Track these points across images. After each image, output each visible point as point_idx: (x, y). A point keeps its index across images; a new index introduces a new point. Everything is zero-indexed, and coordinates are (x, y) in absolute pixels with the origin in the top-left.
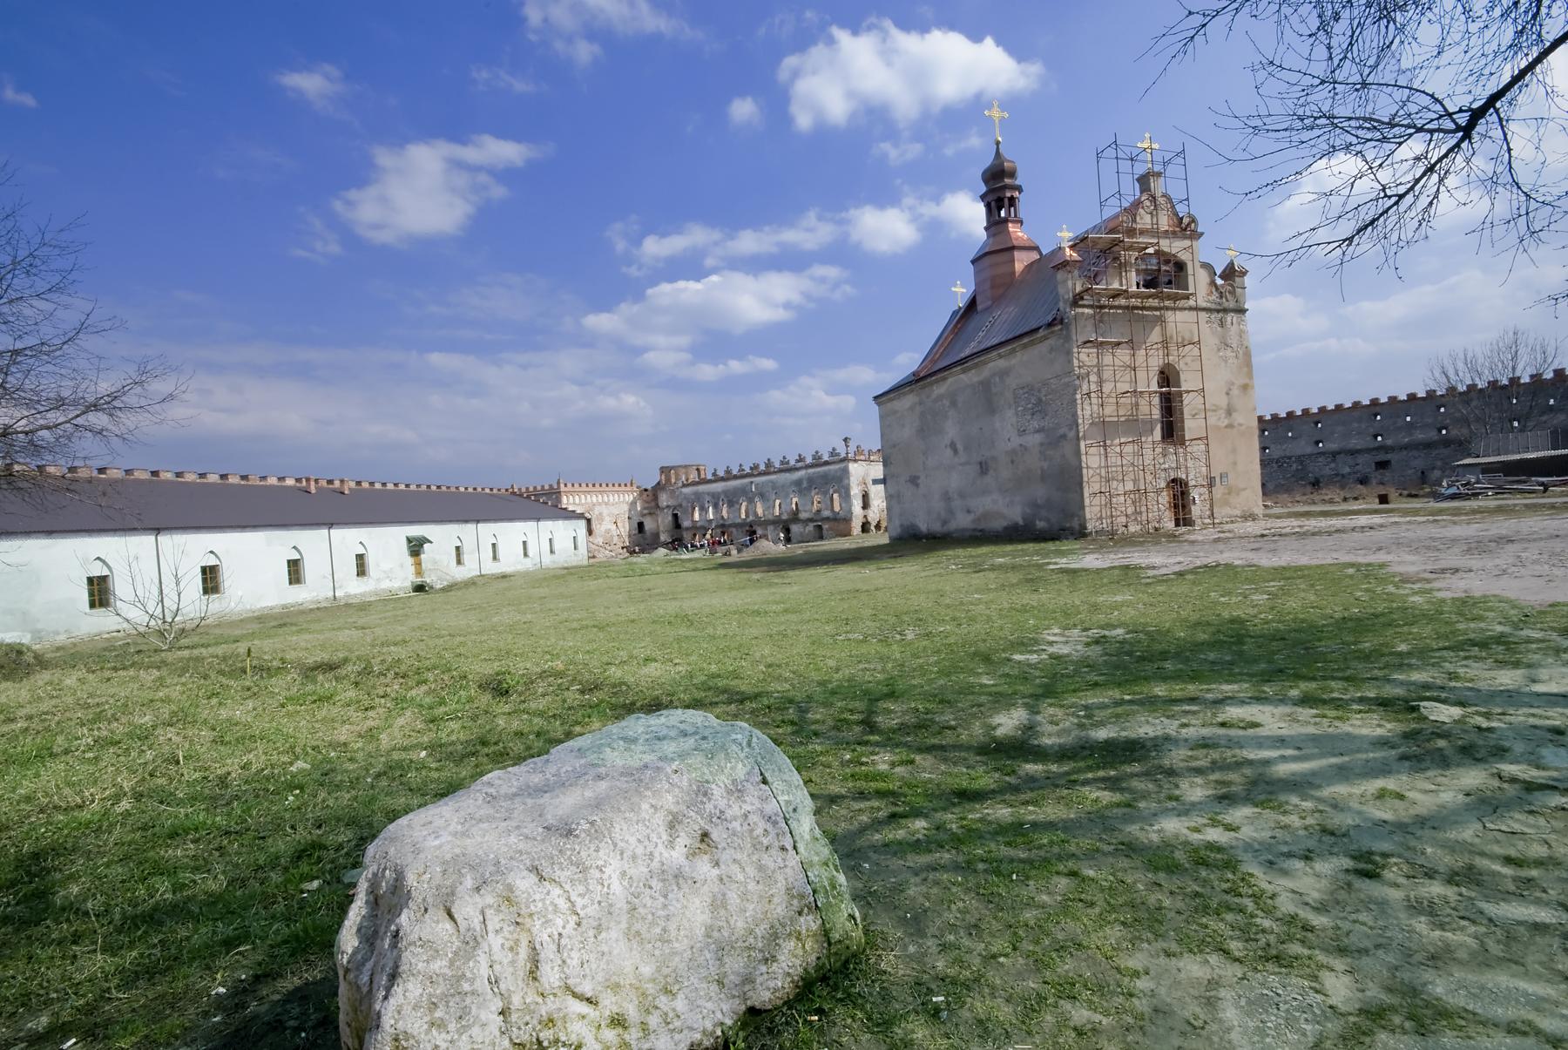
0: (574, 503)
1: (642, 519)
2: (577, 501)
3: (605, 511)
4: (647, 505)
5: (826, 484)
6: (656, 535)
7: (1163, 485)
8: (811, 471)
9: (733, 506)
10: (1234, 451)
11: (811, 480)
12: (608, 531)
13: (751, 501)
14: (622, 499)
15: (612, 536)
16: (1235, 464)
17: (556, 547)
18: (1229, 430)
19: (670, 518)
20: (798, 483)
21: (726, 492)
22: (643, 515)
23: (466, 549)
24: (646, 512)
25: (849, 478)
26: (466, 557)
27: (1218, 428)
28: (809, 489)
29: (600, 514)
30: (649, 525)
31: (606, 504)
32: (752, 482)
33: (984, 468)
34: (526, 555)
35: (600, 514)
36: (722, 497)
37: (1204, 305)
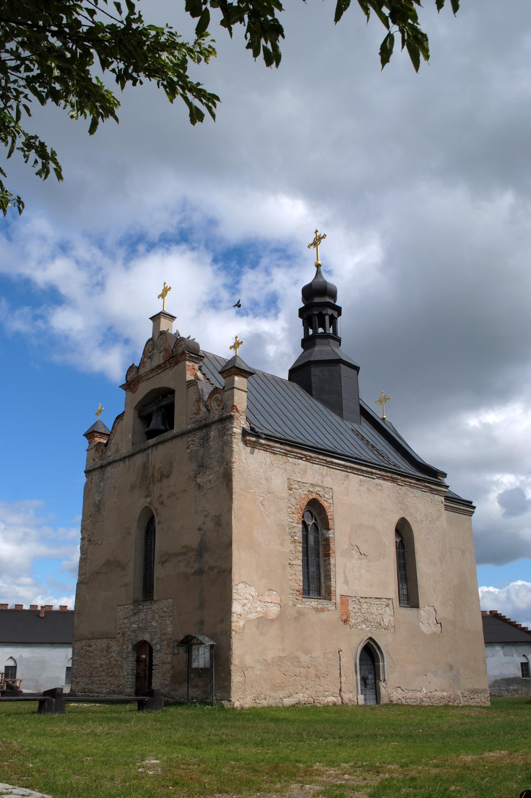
7: (130, 647)
16: (202, 623)
37: (189, 427)
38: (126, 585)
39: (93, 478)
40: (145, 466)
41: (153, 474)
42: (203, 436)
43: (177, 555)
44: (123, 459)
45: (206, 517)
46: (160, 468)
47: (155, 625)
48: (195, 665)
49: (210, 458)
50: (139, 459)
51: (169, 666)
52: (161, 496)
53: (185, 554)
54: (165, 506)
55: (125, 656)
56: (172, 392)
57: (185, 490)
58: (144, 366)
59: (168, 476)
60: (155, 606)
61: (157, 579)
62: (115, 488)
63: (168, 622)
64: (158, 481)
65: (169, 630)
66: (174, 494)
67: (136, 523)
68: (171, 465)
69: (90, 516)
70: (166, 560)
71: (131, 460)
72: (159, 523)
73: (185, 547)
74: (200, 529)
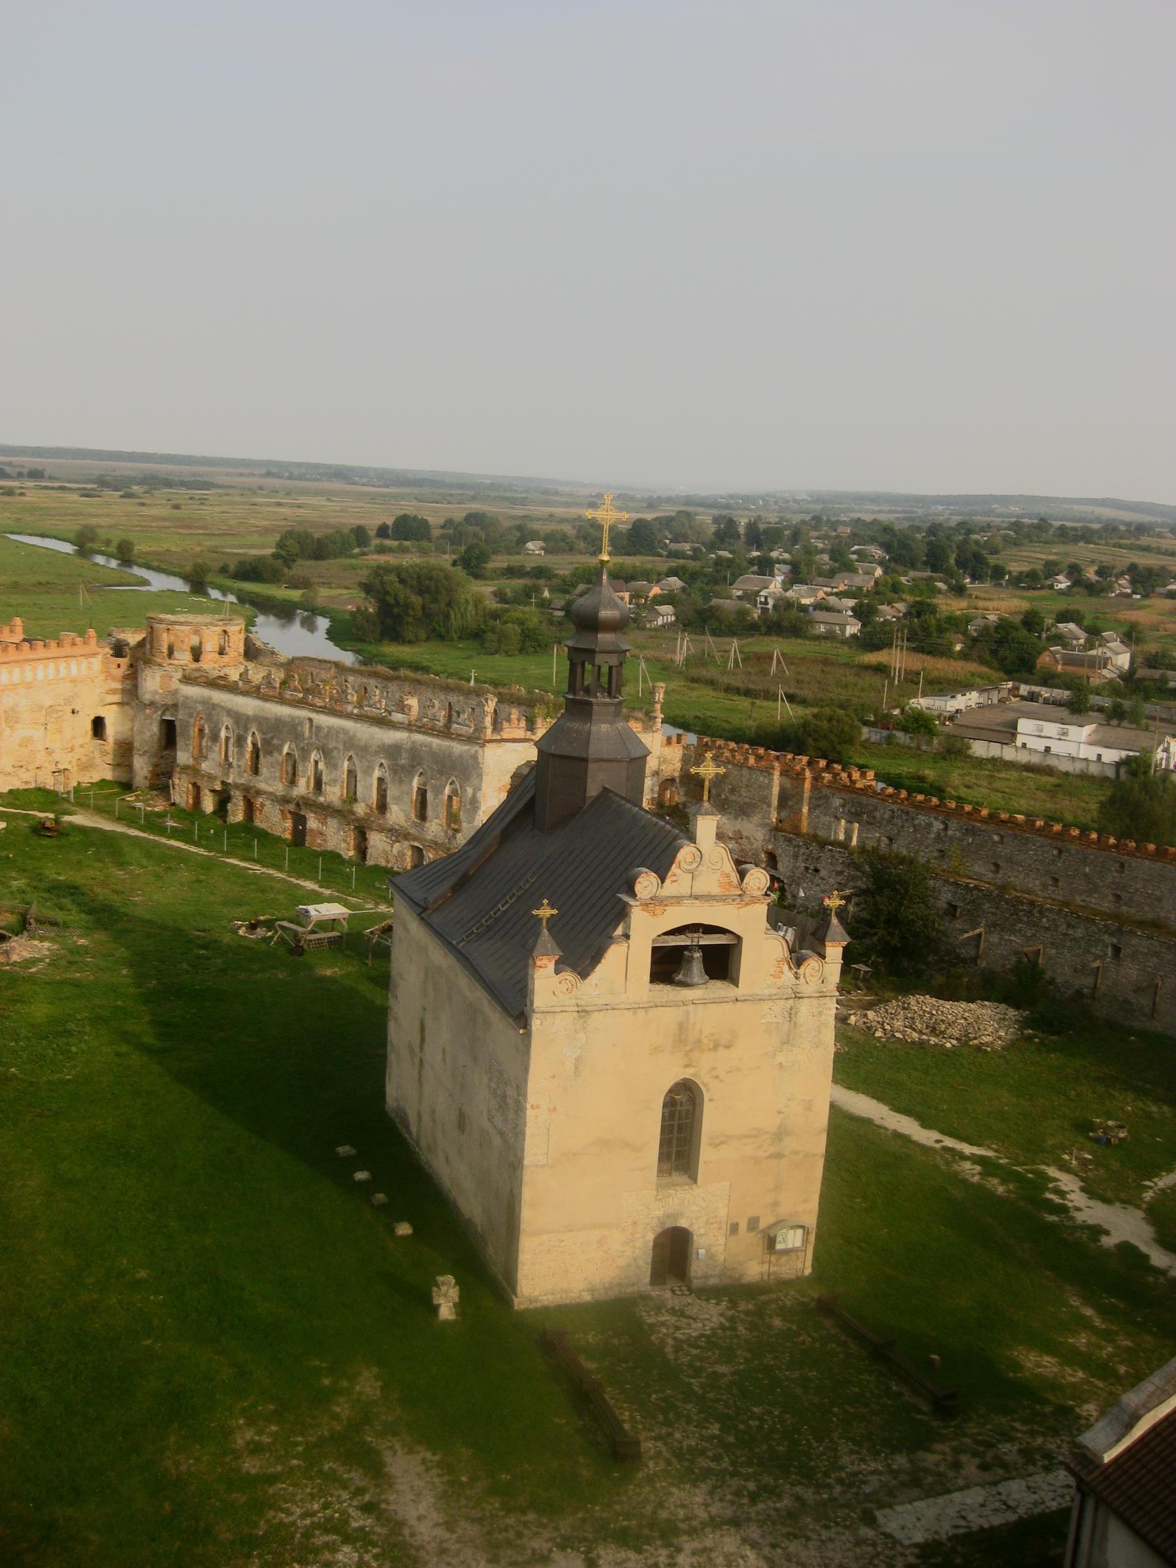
1: (101, 712)
5: (441, 773)
7: (651, 1237)
8: (419, 738)
9: (270, 753)
11: (416, 756)
12: (26, 742)
16: (776, 1204)
19: (155, 728)
20: (392, 751)
21: (263, 722)
25: (480, 776)
28: (409, 771)
31: (29, 686)
32: (310, 720)
36: (254, 729)
37: (765, 992)
38: (644, 1168)
40: (682, 1027)
41: (699, 1041)
42: (789, 1007)
45: (789, 1100)
46: (713, 1034)
47: (697, 1209)
48: (779, 1247)
49: (800, 1037)
50: (669, 1017)
52: (714, 1068)
56: (739, 938)
57: (759, 1067)
58: (675, 881)
59: (727, 1047)
60: (698, 1191)
61: (705, 1163)
62: (614, 1045)
64: (709, 1050)
65: (723, 1212)
66: (738, 1069)
70: (722, 1143)
72: (711, 1100)
74: (779, 1112)
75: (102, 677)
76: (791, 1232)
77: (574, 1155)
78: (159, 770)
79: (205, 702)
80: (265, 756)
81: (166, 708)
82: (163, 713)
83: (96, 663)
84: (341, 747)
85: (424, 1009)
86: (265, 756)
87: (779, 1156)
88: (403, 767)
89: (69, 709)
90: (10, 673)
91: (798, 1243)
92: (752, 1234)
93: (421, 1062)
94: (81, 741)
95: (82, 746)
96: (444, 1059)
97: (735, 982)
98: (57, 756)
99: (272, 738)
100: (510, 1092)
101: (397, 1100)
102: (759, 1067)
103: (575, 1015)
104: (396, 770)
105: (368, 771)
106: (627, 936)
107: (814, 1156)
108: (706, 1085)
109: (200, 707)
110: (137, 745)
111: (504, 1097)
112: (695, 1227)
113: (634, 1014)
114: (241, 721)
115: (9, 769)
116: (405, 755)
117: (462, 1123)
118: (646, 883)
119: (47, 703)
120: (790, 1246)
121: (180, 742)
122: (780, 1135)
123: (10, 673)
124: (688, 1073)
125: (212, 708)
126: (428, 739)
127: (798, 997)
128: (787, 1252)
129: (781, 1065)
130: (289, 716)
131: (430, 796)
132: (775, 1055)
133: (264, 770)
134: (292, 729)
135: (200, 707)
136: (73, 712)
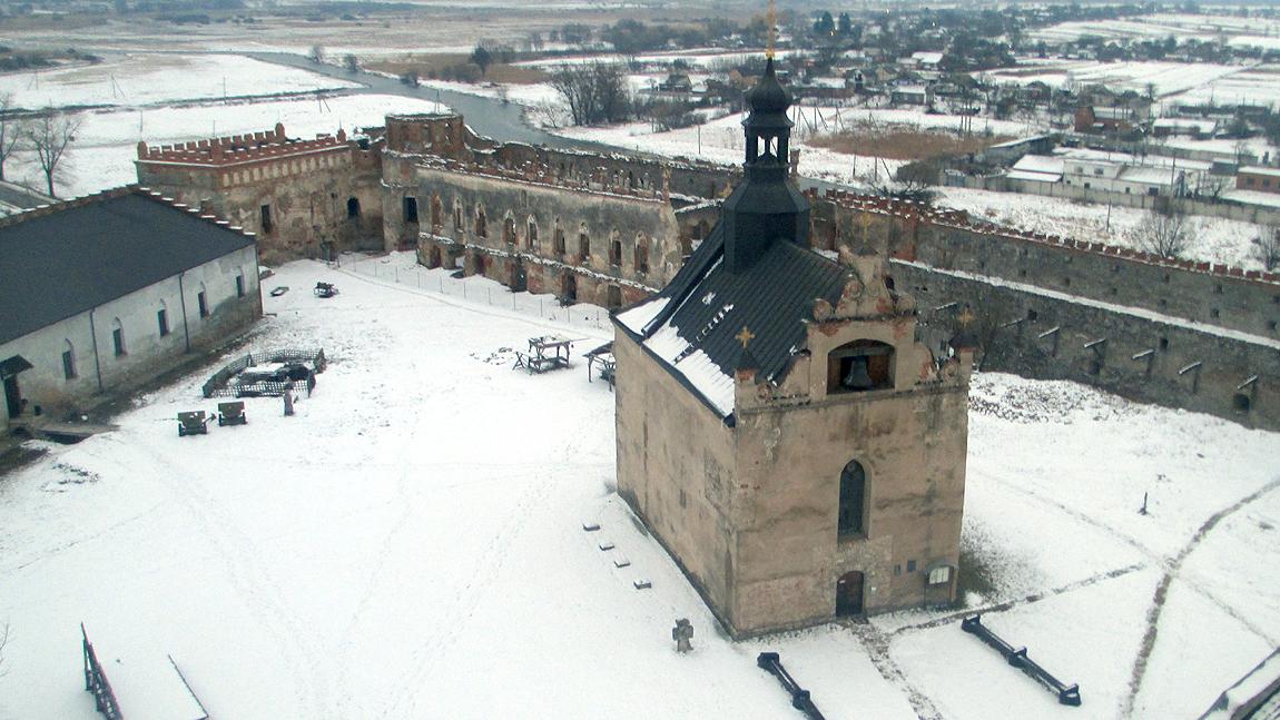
0: (240, 186)
2: (246, 178)
3: (293, 190)
4: (365, 173)
5: (632, 228)
6: (377, 222)
7: (835, 579)
9: (495, 220)
10: (929, 537)
13: (522, 219)
14: (322, 164)
15: (304, 230)
16: (927, 550)
17: (213, 302)
18: (925, 519)
19: (400, 205)
20: (591, 213)
22: (356, 187)
23: (77, 353)
24: (360, 183)
26: (78, 366)
27: (911, 517)
28: (606, 227)
29: (286, 196)
30: (367, 203)
31: (295, 177)
32: (524, 192)
33: (683, 500)
34: (164, 331)
35: (286, 196)
39: (758, 421)
40: (853, 421)
41: (867, 429)
43: (899, 501)
44: (817, 406)
48: (932, 582)
50: (842, 411)
51: (888, 586)
52: (879, 449)
53: (910, 500)
54: (884, 459)
55: (827, 585)
56: (891, 350)
59: (888, 433)
61: (874, 521)
63: (886, 552)
65: (888, 558)
66: (897, 449)
67: (839, 476)
68: (893, 422)
69: (757, 463)
70: (885, 507)
71: (829, 410)
72: (877, 473)
73: (911, 494)
74: (929, 480)
75: (353, 167)
76: (940, 571)
77: (776, 521)
78: (404, 238)
79: (440, 182)
80: (490, 222)
81: (407, 189)
82: (405, 194)
83: (348, 157)
84: (551, 212)
85: (646, 414)
86: (490, 222)
87: (929, 513)
88: (601, 224)
89: (328, 194)
90: (280, 168)
91: (946, 579)
92: (910, 574)
93: (646, 454)
94: (341, 218)
95: (342, 222)
96: (665, 453)
97: (893, 387)
98: (323, 232)
99: (495, 208)
100: (724, 477)
101: (627, 484)
102: (911, 447)
103: (770, 415)
104: (593, 228)
105: (573, 229)
106: (807, 352)
107: (955, 512)
108: (872, 462)
109: (435, 187)
110: (386, 218)
111: (718, 480)
112: (868, 570)
113: (817, 411)
114: (468, 195)
115: (286, 244)
116: (600, 215)
117: (683, 500)
118: (823, 310)
119: (311, 192)
120: (939, 581)
121: (623, 259)
122: (930, 497)
123: (280, 168)
124: (857, 455)
125: (445, 188)
126: (619, 202)
127: (940, 392)
128: (937, 585)
129: (928, 444)
130: (508, 189)
131: (622, 245)
132: (924, 436)
133: (490, 233)
134: (510, 199)
135: (435, 187)
136: (333, 195)
